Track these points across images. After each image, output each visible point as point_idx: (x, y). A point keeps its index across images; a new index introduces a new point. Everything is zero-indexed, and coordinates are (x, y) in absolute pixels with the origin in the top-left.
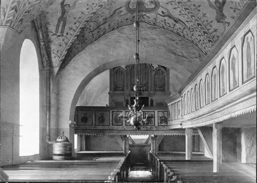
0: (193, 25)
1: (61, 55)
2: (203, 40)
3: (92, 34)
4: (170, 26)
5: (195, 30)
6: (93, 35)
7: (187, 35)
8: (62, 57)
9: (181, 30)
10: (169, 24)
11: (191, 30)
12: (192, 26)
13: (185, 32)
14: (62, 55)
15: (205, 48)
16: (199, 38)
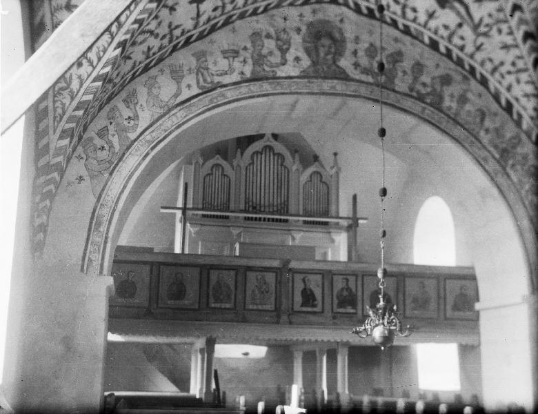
0: (494, 13)
1: (99, 59)
2: (513, 64)
3: (194, 14)
4: (414, 20)
5: (494, 32)
6: (198, 15)
7: (462, 48)
8: (104, 67)
9: (445, 33)
10: (414, 10)
11: (483, 29)
12: (490, 15)
13: (456, 40)
14: (104, 60)
15: (509, 89)
16: (499, 55)
